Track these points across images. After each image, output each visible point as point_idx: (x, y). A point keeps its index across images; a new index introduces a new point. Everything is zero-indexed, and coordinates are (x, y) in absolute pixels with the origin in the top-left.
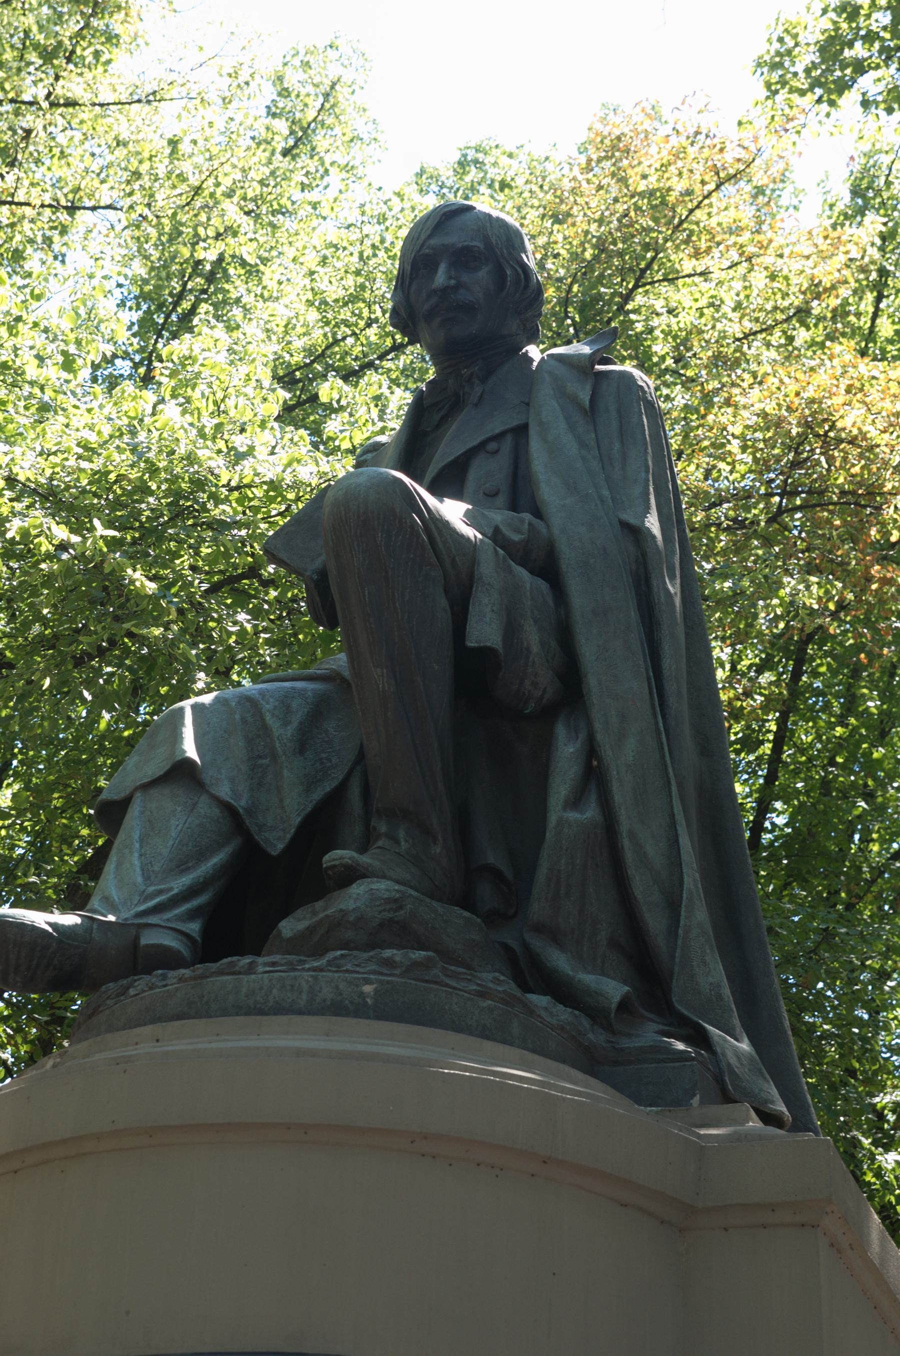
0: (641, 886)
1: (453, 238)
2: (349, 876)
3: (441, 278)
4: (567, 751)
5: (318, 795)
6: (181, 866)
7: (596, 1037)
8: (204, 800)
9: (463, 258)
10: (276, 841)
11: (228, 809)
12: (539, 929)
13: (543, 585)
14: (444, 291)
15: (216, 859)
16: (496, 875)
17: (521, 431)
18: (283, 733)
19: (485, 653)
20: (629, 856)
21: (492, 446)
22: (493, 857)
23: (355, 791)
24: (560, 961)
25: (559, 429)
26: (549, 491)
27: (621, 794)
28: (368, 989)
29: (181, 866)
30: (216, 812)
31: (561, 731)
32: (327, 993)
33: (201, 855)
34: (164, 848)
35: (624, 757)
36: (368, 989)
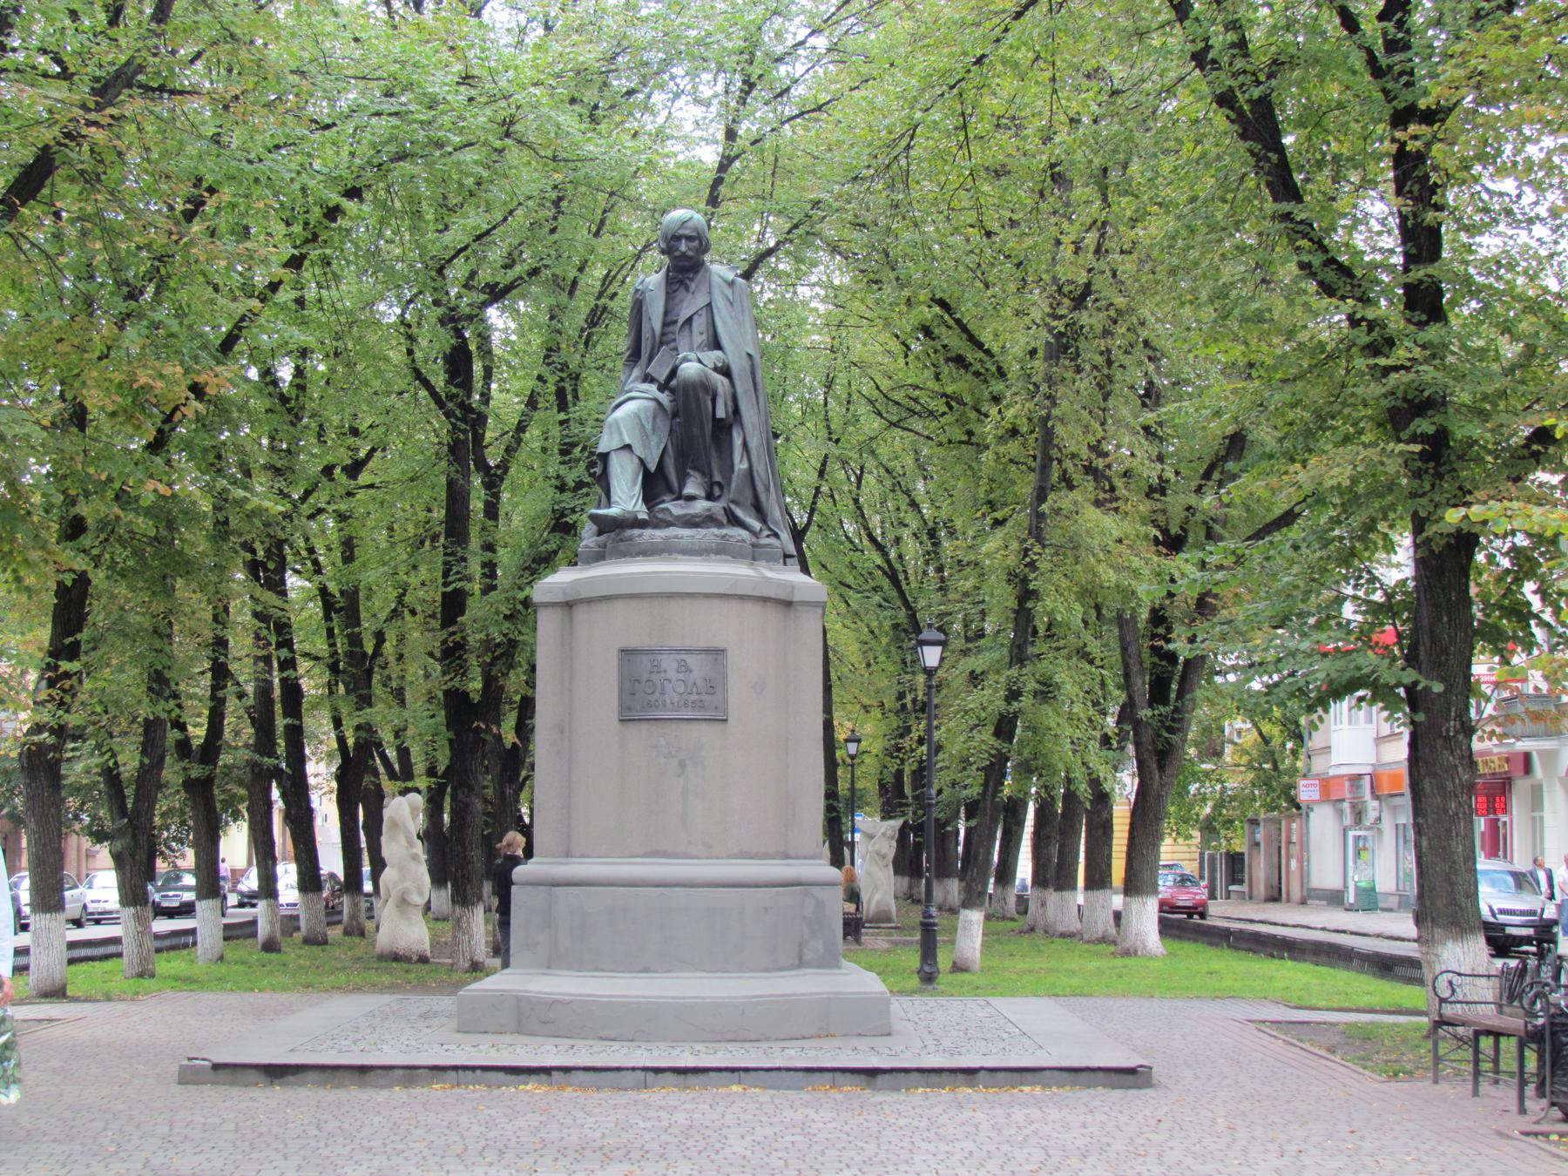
0: (760, 488)
1: (687, 232)
2: (691, 498)
4: (738, 441)
6: (634, 484)
7: (754, 540)
9: (689, 238)
10: (652, 467)
11: (641, 461)
12: (733, 502)
13: (725, 381)
16: (719, 484)
17: (709, 305)
18: (649, 427)
22: (717, 478)
24: (739, 513)
25: (725, 312)
26: (725, 341)
27: (754, 459)
29: (634, 484)
31: (735, 434)
34: (629, 476)
35: (753, 444)
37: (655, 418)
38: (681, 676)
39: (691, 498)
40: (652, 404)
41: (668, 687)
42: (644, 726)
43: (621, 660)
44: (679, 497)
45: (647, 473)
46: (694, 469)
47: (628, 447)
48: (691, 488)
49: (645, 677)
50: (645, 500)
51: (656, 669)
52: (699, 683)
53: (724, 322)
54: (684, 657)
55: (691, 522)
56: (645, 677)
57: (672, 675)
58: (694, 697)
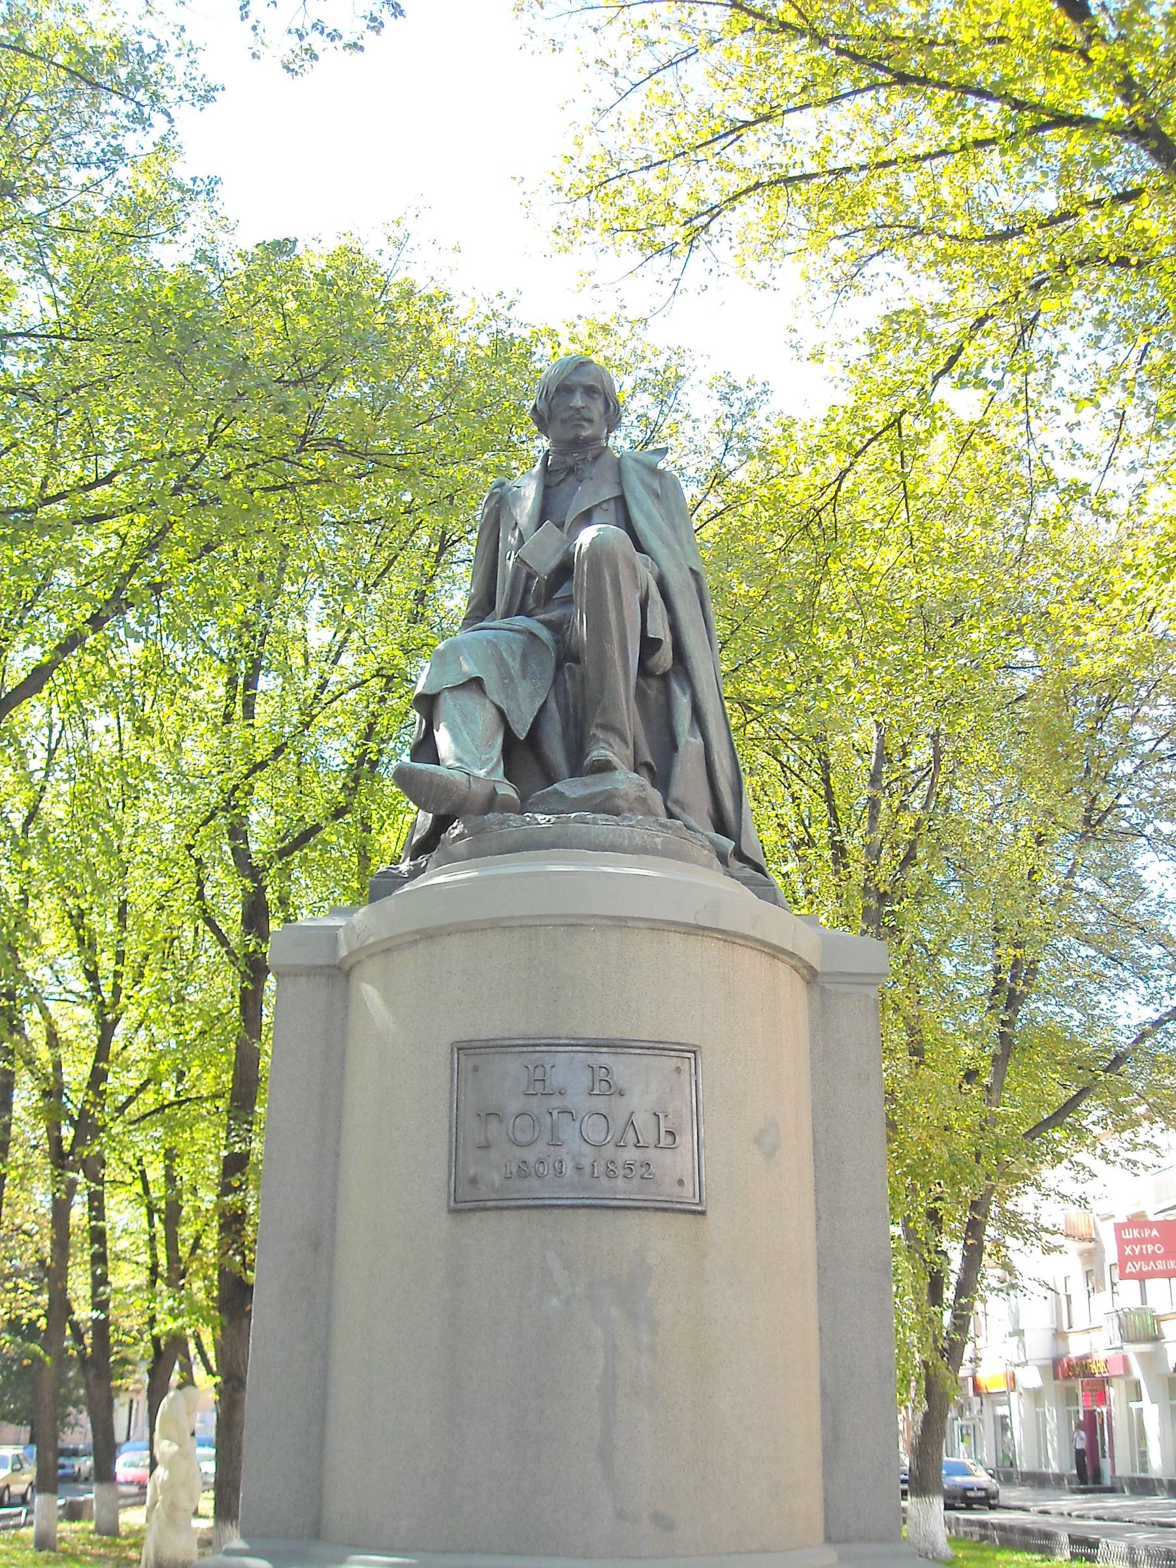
2: (605, 767)
3: (578, 400)
4: (683, 702)
5: (537, 705)
8: (488, 705)
11: (500, 710)
14: (578, 410)
15: (500, 740)
17: (621, 501)
18: (515, 665)
19: (658, 643)
20: (717, 766)
21: (605, 506)
23: (552, 705)
25: (649, 503)
28: (658, 840)
30: (494, 710)
31: (676, 688)
32: (638, 841)
33: (493, 737)
36: (658, 840)
37: (524, 658)
38: (601, 1104)
39: (605, 767)
40: (517, 636)
41: (569, 1132)
42: (510, 1219)
43: (457, 1072)
44: (576, 770)
45: (509, 737)
46: (606, 727)
47: (476, 683)
48: (597, 753)
49: (514, 1106)
50: (507, 774)
51: (539, 1085)
52: (643, 1120)
53: (649, 517)
54: (606, 1059)
55: (606, 805)
56: (514, 1106)
57: (578, 1100)
58: (630, 1154)
